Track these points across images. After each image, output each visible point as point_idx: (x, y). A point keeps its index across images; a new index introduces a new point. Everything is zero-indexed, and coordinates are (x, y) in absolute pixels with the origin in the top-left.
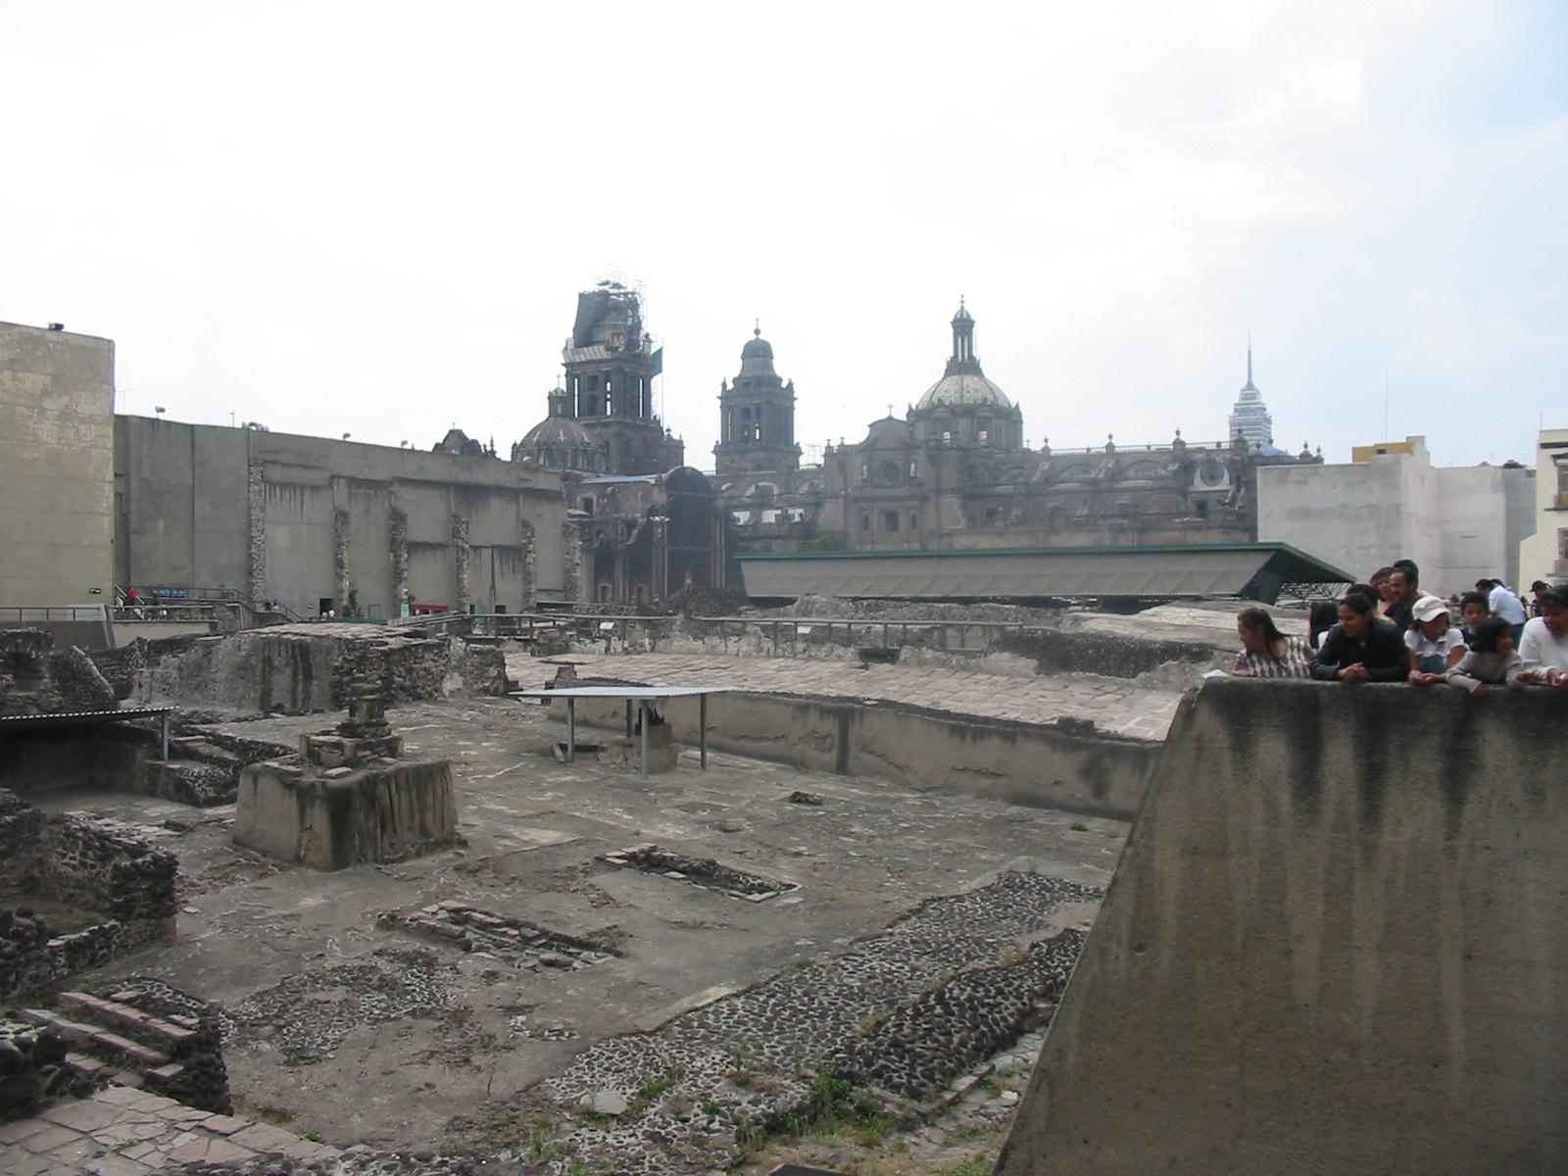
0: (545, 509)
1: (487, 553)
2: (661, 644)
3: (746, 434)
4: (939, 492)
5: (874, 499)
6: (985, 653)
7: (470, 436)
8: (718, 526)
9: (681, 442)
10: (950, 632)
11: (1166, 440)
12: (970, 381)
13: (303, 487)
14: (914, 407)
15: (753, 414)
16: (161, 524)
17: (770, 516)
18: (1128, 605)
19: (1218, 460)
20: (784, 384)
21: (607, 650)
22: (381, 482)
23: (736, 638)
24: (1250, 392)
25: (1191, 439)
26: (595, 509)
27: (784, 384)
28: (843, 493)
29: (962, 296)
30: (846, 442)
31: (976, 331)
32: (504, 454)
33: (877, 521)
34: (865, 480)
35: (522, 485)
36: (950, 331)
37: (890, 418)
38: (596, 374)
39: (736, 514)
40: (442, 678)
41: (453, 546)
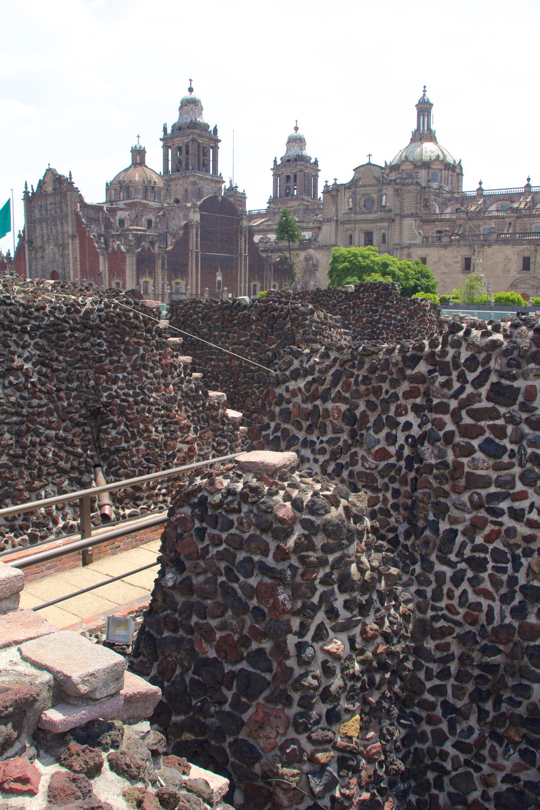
3: (288, 191)
4: (403, 217)
5: (356, 222)
8: (243, 239)
9: (244, 194)
14: (388, 163)
15: (292, 178)
20: (313, 161)
27: (313, 161)
28: (335, 218)
29: (425, 87)
30: (338, 182)
31: (433, 111)
34: (350, 209)
36: (414, 112)
37: (369, 164)
38: (181, 145)
39: (269, 236)
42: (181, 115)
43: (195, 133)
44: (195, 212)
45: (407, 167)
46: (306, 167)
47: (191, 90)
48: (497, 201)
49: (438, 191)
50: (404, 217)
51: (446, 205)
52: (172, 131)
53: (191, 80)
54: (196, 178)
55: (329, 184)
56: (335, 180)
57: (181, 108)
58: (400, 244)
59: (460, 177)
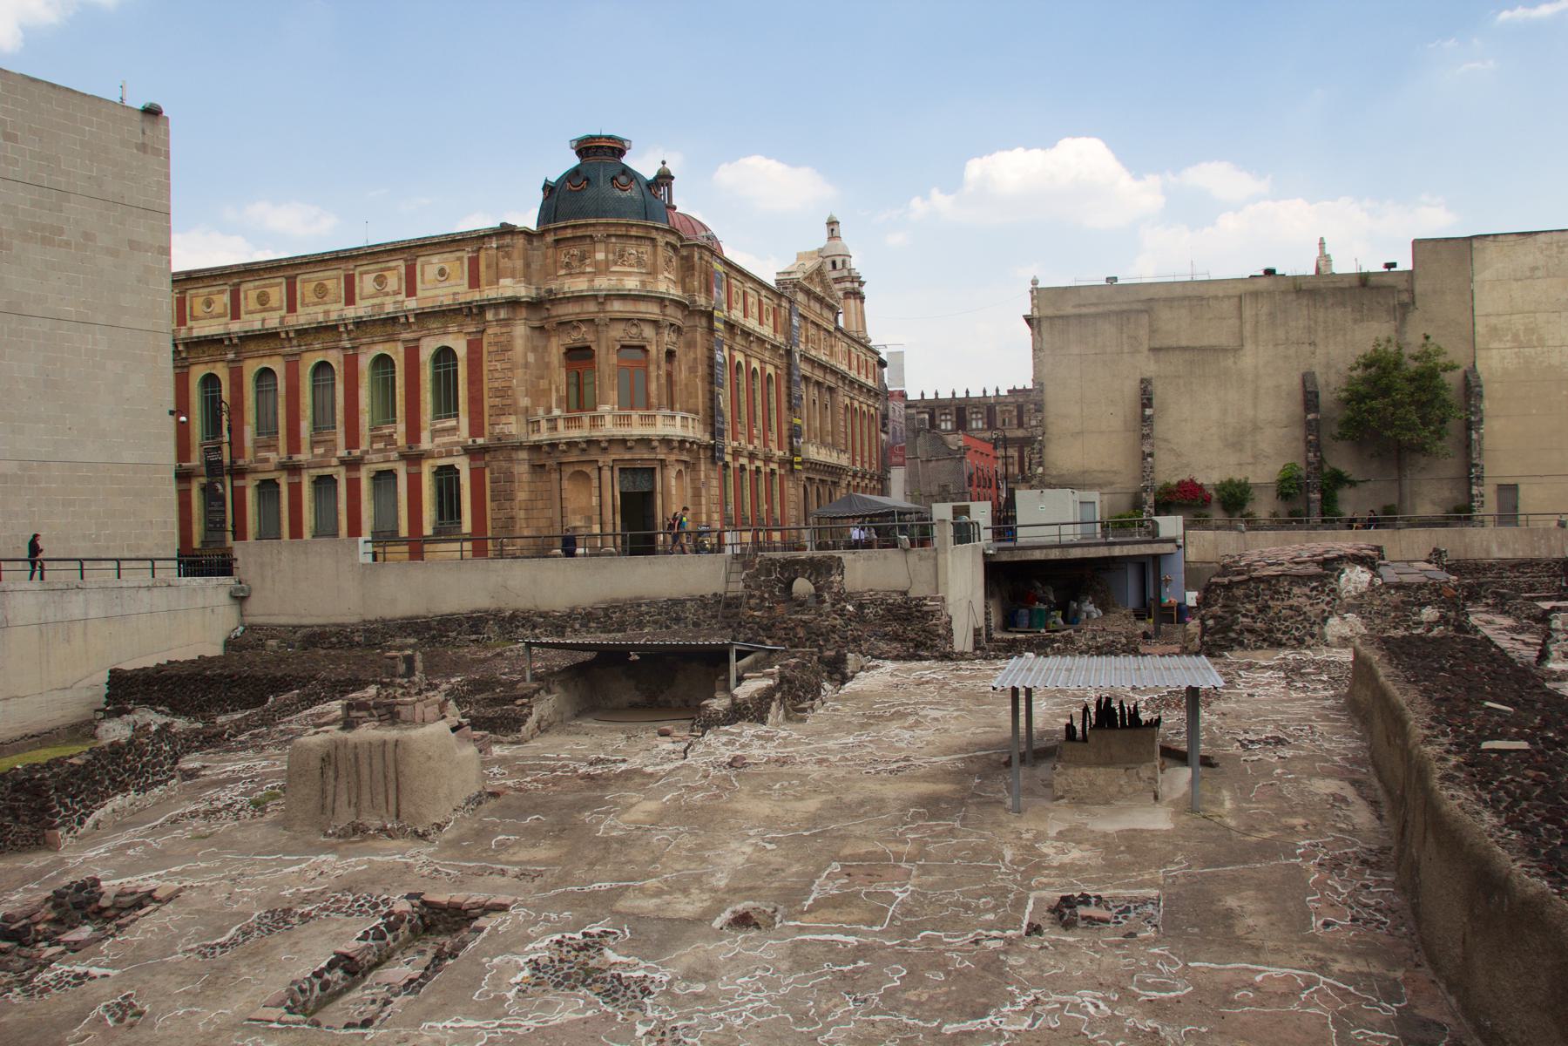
40: (1325, 620)
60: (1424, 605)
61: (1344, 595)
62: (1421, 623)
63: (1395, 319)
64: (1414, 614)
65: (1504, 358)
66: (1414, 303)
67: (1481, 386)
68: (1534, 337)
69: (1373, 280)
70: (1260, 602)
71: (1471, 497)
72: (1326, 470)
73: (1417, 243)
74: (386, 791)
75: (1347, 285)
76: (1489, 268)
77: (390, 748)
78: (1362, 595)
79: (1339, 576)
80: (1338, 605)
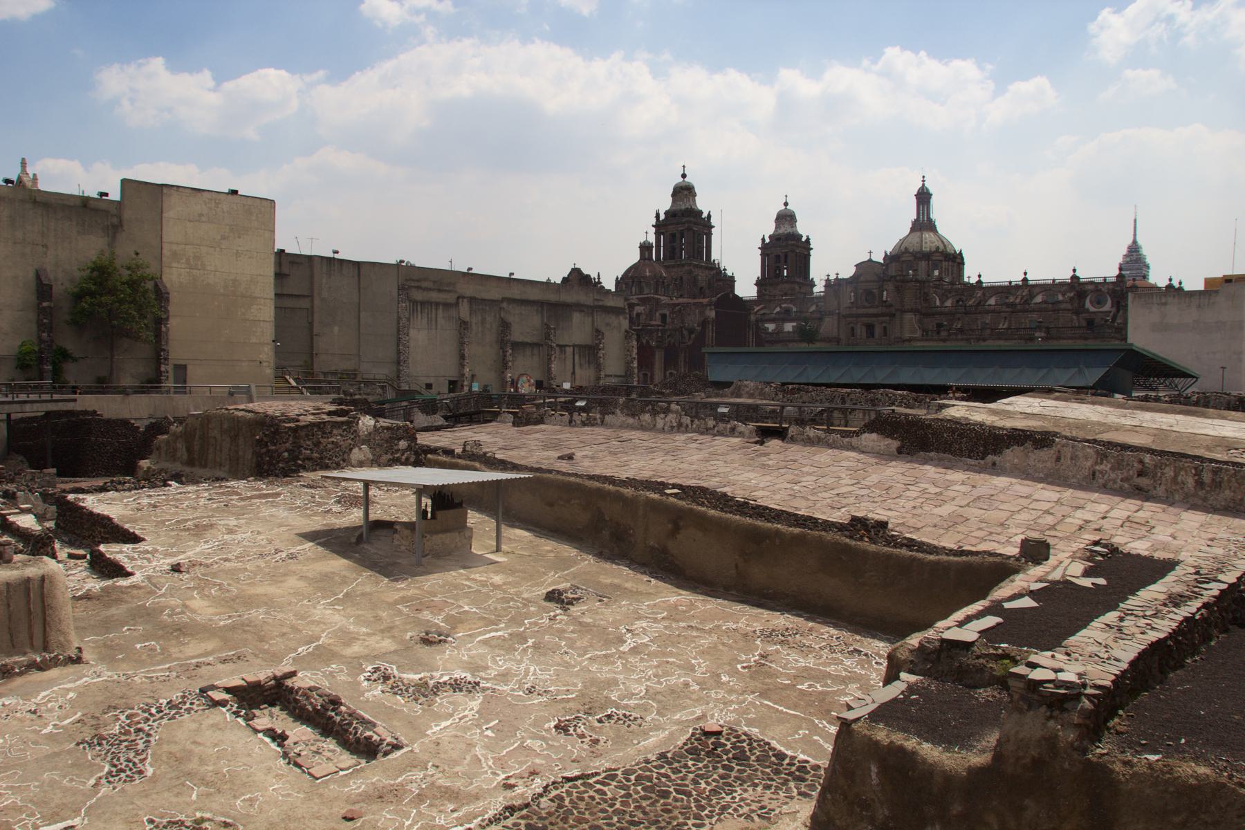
0: (612, 319)
1: (569, 350)
2: (608, 418)
4: (904, 311)
5: (858, 316)
6: (857, 434)
7: (585, 272)
10: (836, 414)
11: (1065, 275)
12: (928, 236)
13: (437, 304)
14: (888, 253)
15: (782, 259)
16: (336, 329)
17: (789, 327)
18: (988, 395)
19: (1103, 289)
21: (570, 422)
22: (493, 302)
23: (662, 416)
24: (1134, 249)
25: (1085, 274)
26: (668, 320)
29: (924, 177)
30: (840, 277)
31: (934, 201)
32: (609, 284)
33: (860, 331)
34: (852, 303)
35: (596, 303)
36: (915, 201)
37: (870, 260)
39: (766, 325)
41: (543, 346)
42: (674, 202)
43: (690, 222)
44: (711, 309)
45: (906, 258)
46: (798, 247)
47: (684, 176)
48: (996, 294)
49: (937, 283)
50: (905, 311)
51: (946, 296)
52: (666, 218)
53: (684, 167)
54: (692, 267)
55: (830, 278)
56: (837, 274)
57: (673, 195)
58: (900, 338)
59: (961, 266)
60: (400, 439)
61: (361, 434)
62: (398, 450)
63: (108, 236)
64: (396, 445)
65: (180, 275)
66: (121, 226)
67: (168, 293)
68: (199, 263)
69: (91, 202)
70: (315, 440)
71: (159, 373)
72: (54, 347)
73: (125, 183)
74: (30, 627)
75: (72, 204)
76: (173, 209)
77: (34, 587)
78: (370, 434)
79: (358, 423)
80: (357, 440)
